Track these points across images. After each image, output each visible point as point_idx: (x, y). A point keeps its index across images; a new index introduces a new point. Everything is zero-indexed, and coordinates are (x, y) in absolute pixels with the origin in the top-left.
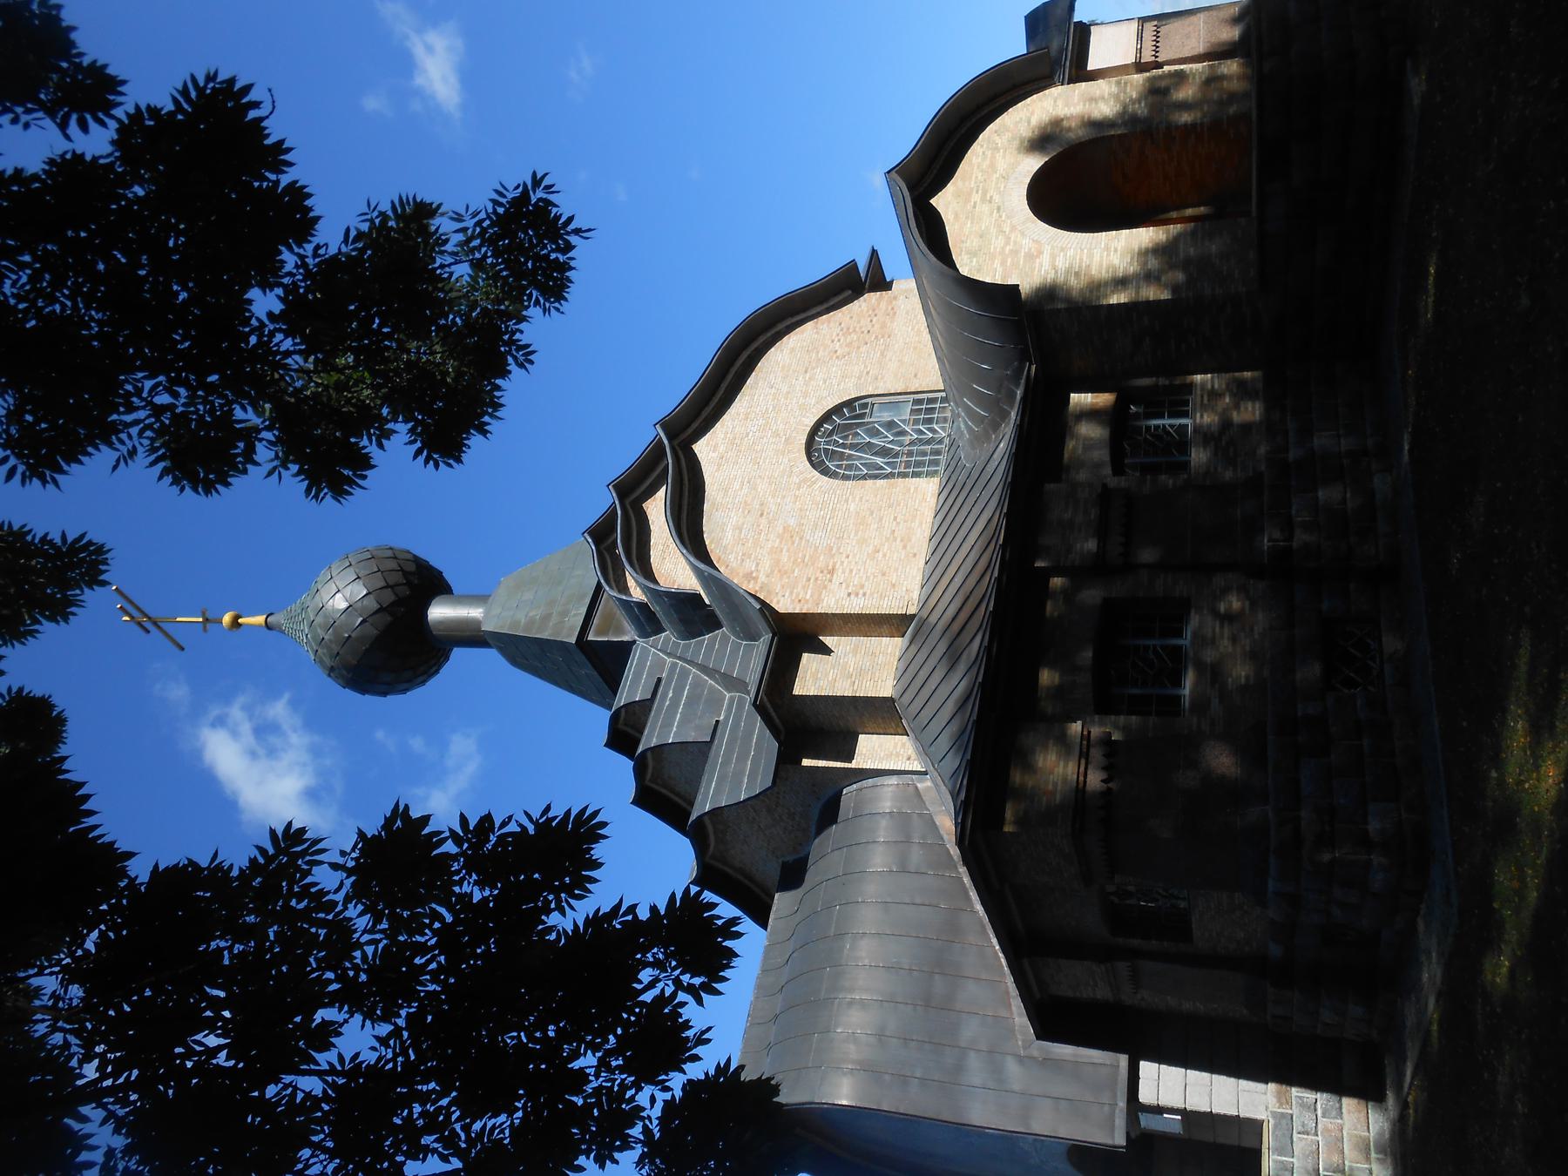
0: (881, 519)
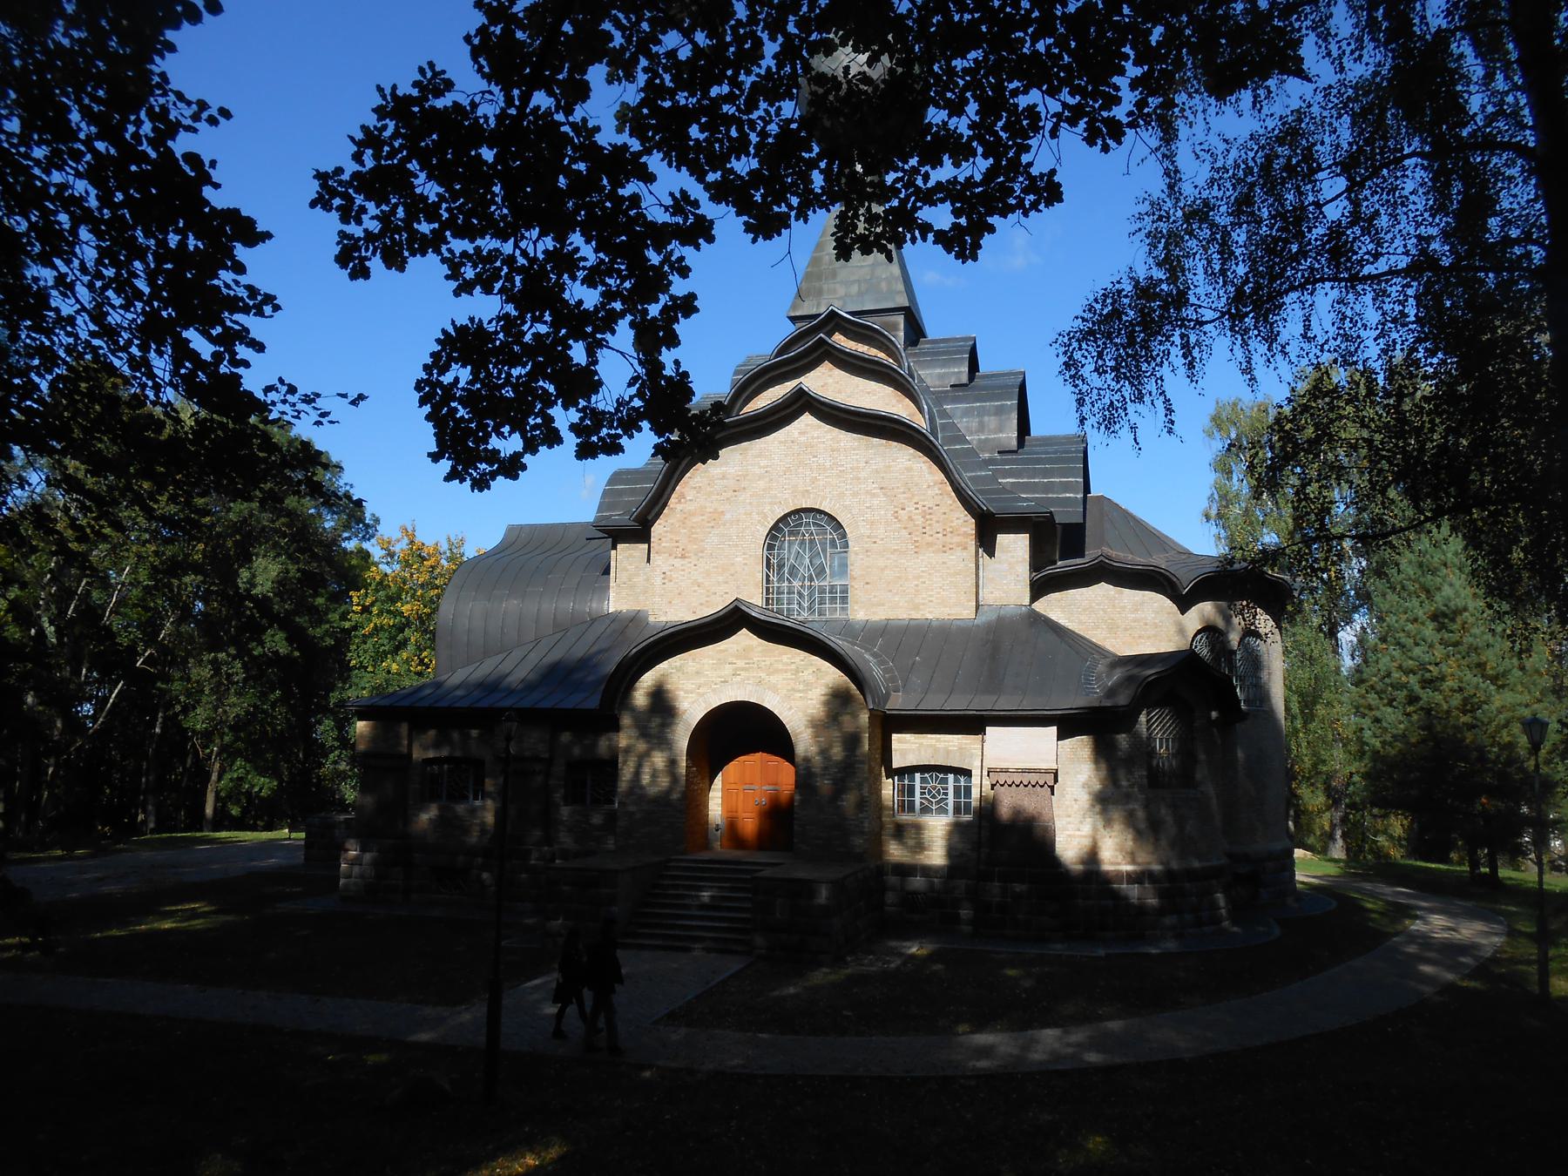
0: (726, 583)
